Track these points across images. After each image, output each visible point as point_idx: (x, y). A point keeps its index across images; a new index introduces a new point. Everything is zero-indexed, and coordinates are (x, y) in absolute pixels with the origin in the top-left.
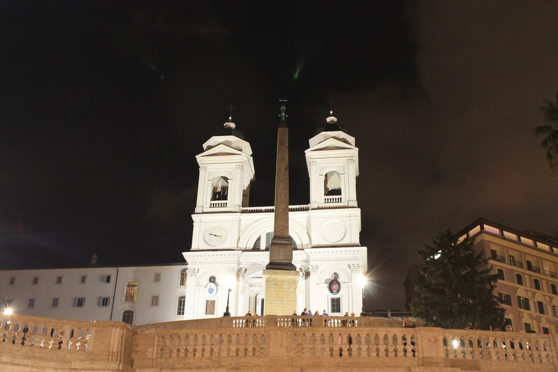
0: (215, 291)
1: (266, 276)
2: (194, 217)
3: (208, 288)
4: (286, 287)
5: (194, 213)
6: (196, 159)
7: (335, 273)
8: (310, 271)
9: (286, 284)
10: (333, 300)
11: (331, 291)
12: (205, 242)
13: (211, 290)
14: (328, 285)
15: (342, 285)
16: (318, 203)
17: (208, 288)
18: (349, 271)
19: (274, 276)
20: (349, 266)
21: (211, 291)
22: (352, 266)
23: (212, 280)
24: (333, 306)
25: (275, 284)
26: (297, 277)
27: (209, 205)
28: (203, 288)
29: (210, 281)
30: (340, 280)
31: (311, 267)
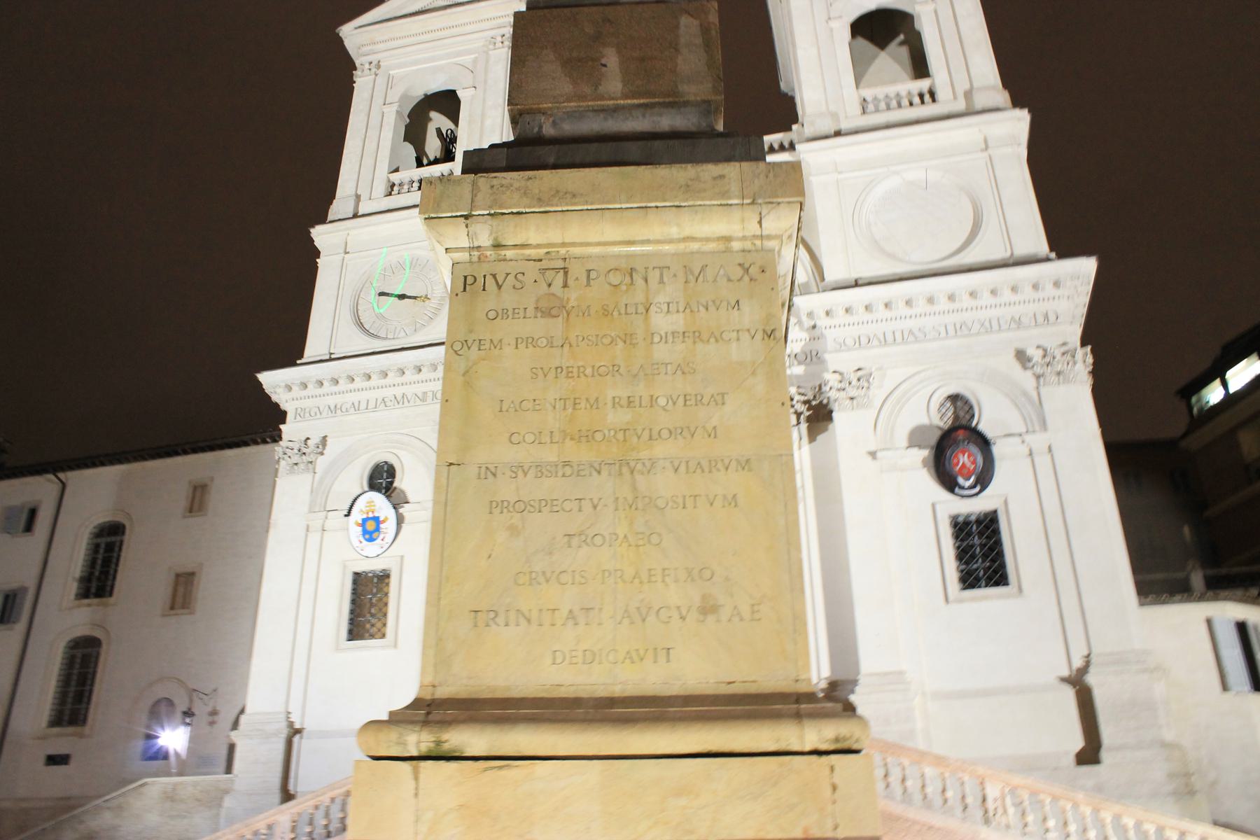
0: (389, 527)
1: (458, 236)
2: (320, 234)
3: (357, 515)
4: (662, 322)
5: (322, 219)
6: (340, 41)
7: (955, 398)
8: (833, 394)
9: (670, 292)
10: (961, 528)
11: (948, 482)
12: (361, 325)
13: (371, 526)
14: (925, 453)
15: (996, 450)
16: (834, 116)
17: (357, 515)
18: (1026, 379)
19: (537, 234)
20: (1022, 357)
21: (371, 528)
22: (1036, 355)
23: (382, 479)
24: (964, 555)
25: (546, 311)
26: (780, 221)
27: (380, 188)
28: (336, 519)
29: (373, 486)
30: (985, 425)
31: (832, 379)
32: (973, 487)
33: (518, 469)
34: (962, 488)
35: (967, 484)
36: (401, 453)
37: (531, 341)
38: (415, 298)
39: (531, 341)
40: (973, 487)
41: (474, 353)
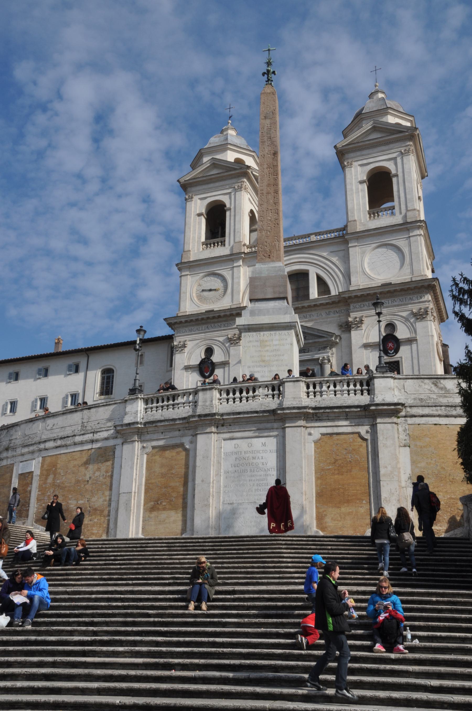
32: (393, 353)
33: (253, 367)
34: (390, 354)
35: (391, 352)
36: (213, 346)
37: (255, 346)
38: (215, 290)
39: (255, 346)
40: (393, 353)
41: (246, 348)
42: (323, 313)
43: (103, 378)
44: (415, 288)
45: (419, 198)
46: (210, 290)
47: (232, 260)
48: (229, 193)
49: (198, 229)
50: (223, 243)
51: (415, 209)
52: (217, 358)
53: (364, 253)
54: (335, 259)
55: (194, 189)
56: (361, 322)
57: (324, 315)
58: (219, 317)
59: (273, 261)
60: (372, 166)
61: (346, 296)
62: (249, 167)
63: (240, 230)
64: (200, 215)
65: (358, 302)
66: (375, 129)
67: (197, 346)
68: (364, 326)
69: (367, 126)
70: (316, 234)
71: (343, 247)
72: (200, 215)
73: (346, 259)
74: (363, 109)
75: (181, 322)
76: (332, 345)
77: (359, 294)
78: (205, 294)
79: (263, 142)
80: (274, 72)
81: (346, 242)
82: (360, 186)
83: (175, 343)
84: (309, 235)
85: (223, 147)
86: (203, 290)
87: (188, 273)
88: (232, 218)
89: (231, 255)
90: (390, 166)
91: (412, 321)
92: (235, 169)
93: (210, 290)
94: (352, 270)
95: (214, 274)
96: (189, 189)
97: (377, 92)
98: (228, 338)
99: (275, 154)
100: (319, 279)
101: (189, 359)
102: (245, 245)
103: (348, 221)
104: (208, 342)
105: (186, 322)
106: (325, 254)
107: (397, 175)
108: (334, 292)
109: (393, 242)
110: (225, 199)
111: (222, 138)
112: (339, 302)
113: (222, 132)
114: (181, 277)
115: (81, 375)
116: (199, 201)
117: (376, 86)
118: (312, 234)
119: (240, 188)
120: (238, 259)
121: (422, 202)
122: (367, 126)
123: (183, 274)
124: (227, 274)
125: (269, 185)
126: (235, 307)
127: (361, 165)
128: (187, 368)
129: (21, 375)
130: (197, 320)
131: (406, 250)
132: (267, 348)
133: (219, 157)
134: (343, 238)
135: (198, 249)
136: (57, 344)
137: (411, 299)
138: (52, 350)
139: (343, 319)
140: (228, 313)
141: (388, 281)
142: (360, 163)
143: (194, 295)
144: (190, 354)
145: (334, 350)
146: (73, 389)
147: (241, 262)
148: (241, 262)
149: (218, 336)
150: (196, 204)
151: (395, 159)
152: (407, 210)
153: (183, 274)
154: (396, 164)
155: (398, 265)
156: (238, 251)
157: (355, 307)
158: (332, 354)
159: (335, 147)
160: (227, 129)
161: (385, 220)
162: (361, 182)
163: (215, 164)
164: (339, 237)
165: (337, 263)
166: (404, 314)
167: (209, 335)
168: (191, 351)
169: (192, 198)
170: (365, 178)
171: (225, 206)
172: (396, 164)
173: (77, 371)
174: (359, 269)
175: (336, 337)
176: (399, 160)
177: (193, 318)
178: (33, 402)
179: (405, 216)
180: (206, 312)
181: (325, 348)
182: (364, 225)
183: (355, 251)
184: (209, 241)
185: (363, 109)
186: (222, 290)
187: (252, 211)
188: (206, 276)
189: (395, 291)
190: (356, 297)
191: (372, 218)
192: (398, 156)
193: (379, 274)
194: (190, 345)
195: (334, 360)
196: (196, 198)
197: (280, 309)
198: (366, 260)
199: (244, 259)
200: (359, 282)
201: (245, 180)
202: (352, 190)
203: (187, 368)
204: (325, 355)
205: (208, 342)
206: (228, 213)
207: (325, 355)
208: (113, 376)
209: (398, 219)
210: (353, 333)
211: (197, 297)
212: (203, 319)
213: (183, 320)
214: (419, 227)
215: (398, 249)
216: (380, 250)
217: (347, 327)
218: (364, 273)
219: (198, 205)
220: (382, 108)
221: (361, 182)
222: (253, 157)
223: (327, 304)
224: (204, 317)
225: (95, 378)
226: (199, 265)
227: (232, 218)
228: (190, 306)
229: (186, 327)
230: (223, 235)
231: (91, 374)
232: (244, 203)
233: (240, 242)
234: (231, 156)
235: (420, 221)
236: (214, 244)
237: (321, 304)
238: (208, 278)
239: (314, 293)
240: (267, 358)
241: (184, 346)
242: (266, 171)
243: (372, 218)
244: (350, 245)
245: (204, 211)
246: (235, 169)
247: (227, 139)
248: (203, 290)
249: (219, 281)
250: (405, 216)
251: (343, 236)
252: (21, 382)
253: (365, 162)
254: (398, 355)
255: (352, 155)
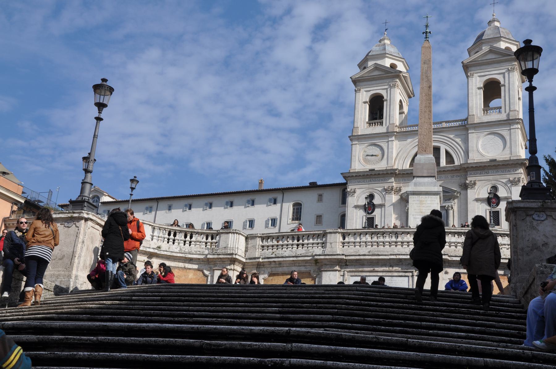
11: (490, 205)
42: (449, 176)
43: (294, 209)
44: (512, 164)
45: (519, 99)
46: (372, 155)
47: (388, 137)
48: (387, 89)
49: (363, 112)
50: (382, 124)
51: (515, 110)
52: (376, 201)
53: (478, 138)
54: (458, 140)
55: (361, 84)
56: (475, 184)
57: (450, 177)
58: (379, 174)
59: (427, 154)
60: (488, 77)
61: (466, 166)
62: (400, 72)
63: (394, 116)
64: (365, 103)
65: (473, 171)
66: (491, 51)
67: (363, 193)
68: (476, 187)
69: (485, 48)
70: (446, 122)
71: (464, 133)
72: (365, 103)
73: (466, 141)
74: (482, 35)
75: (352, 176)
76: (454, 198)
77: (474, 166)
78: (368, 157)
79: (423, 79)
80: (430, 32)
81: (467, 130)
82: (478, 91)
83: (348, 190)
84: (441, 123)
85: (383, 56)
86: (367, 155)
87: (357, 142)
88: (388, 107)
89: (387, 133)
90: (500, 78)
91: (509, 185)
92: (392, 73)
93: (372, 155)
94: (470, 149)
95: (375, 145)
96: (358, 83)
97: (494, 21)
98: (384, 189)
99: (430, 87)
100: (447, 152)
101: (358, 201)
102: (396, 126)
103: (468, 115)
104: (371, 190)
105: (356, 176)
106: (451, 136)
107: (504, 85)
108: (457, 163)
109: (499, 132)
110: (384, 93)
111: (382, 48)
112: (460, 170)
113: (380, 41)
114: (352, 145)
115: (279, 205)
116: (365, 93)
117: (493, 15)
118: (443, 122)
119: (394, 86)
120: (392, 136)
121: (521, 102)
122: (485, 48)
123: (354, 143)
124: (384, 145)
125: (426, 107)
126: (389, 168)
127: (480, 76)
128: (356, 207)
129: (234, 203)
130: (364, 175)
131: (507, 138)
132: (424, 205)
133: (379, 62)
134: (465, 127)
135: (364, 127)
136: (261, 183)
137: (509, 171)
138: (257, 188)
139: (463, 181)
140: (385, 172)
141: (494, 158)
142: (479, 74)
143: (361, 158)
144: (359, 197)
145: (456, 201)
146: (273, 216)
147: (393, 138)
148: (393, 138)
149: (377, 187)
150: (363, 95)
151: (504, 74)
152: (510, 110)
153: (354, 143)
154: (504, 77)
155: (502, 147)
156: (392, 130)
157: (471, 174)
158: (454, 204)
159: (462, 62)
160: (384, 39)
161: (493, 116)
162: (479, 88)
163: (377, 67)
164: (462, 126)
165: (460, 143)
166: (504, 181)
167: (371, 186)
168: (358, 196)
169: (360, 90)
170: (482, 86)
171: (382, 97)
172: (504, 77)
173: (275, 203)
174: (475, 149)
175: (458, 192)
176: (506, 74)
177: (361, 174)
178: (244, 223)
179: (508, 115)
180: (370, 170)
181: (450, 199)
182: (480, 118)
183: (473, 136)
184: (371, 122)
185: (482, 35)
186: (380, 156)
187: (401, 101)
188: (369, 145)
189: (498, 165)
190: (472, 167)
191: (485, 114)
192: (506, 71)
193: (488, 153)
194: (358, 191)
195: (455, 208)
196: (362, 90)
197: (432, 183)
198: (480, 143)
199: (396, 136)
200: (474, 158)
201: (398, 80)
202: (472, 93)
203: (356, 207)
204: (450, 204)
205: (371, 190)
206: (385, 103)
207: (450, 204)
208: (301, 208)
209: (503, 116)
210: (469, 191)
211: (363, 159)
212: (367, 175)
213: (354, 175)
214: (518, 123)
215: (502, 137)
216: (489, 136)
217: (465, 187)
218: (478, 151)
219: (364, 96)
220: (497, 36)
221: (479, 88)
222: (403, 62)
223: (452, 170)
224: (369, 173)
225: (288, 208)
226: (365, 138)
227: (388, 107)
228: (359, 165)
229: (356, 179)
230: (381, 117)
231: (285, 205)
232: (396, 96)
233: (394, 124)
234: (387, 62)
235: (519, 119)
236: (375, 123)
237: (448, 170)
238: (371, 147)
239: (443, 162)
240: (423, 211)
241: (354, 192)
242: (424, 98)
243: (485, 114)
244: (469, 132)
245: (368, 100)
246: (392, 73)
247: (385, 49)
248: (367, 155)
249: (378, 149)
250: (508, 115)
251: (465, 125)
252: (235, 208)
253: (483, 74)
254: (498, 207)
255: (473, 68)
